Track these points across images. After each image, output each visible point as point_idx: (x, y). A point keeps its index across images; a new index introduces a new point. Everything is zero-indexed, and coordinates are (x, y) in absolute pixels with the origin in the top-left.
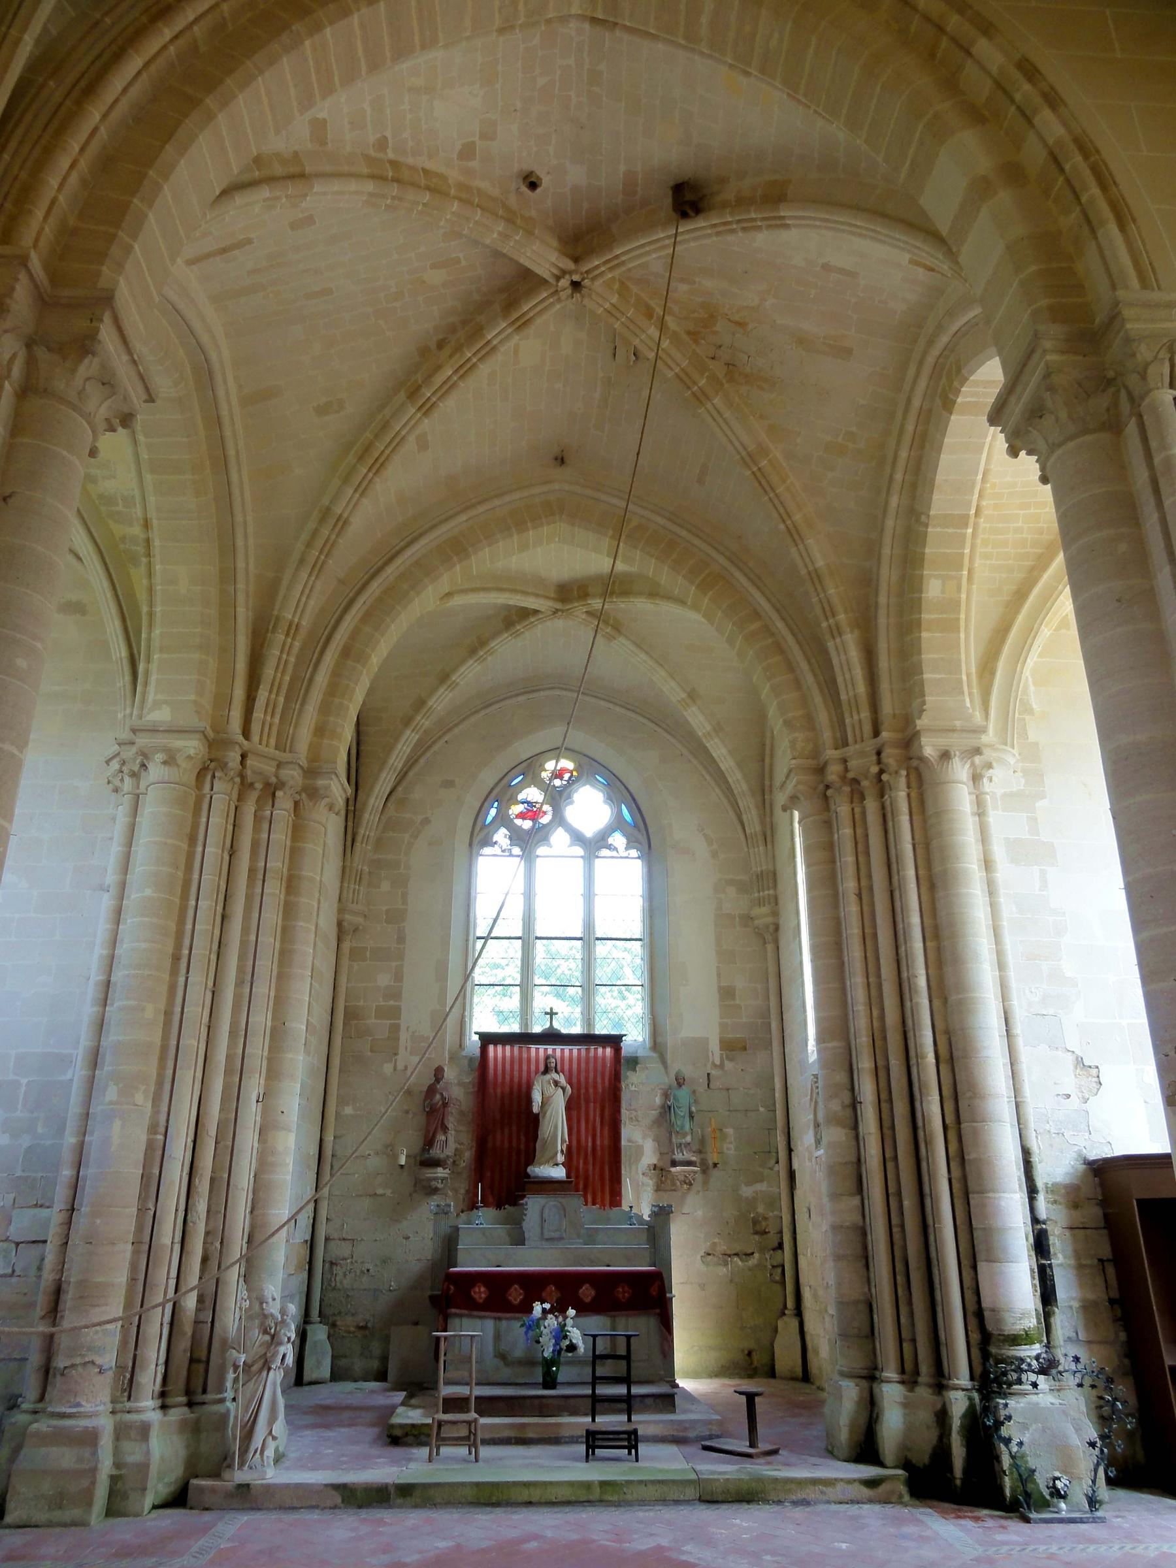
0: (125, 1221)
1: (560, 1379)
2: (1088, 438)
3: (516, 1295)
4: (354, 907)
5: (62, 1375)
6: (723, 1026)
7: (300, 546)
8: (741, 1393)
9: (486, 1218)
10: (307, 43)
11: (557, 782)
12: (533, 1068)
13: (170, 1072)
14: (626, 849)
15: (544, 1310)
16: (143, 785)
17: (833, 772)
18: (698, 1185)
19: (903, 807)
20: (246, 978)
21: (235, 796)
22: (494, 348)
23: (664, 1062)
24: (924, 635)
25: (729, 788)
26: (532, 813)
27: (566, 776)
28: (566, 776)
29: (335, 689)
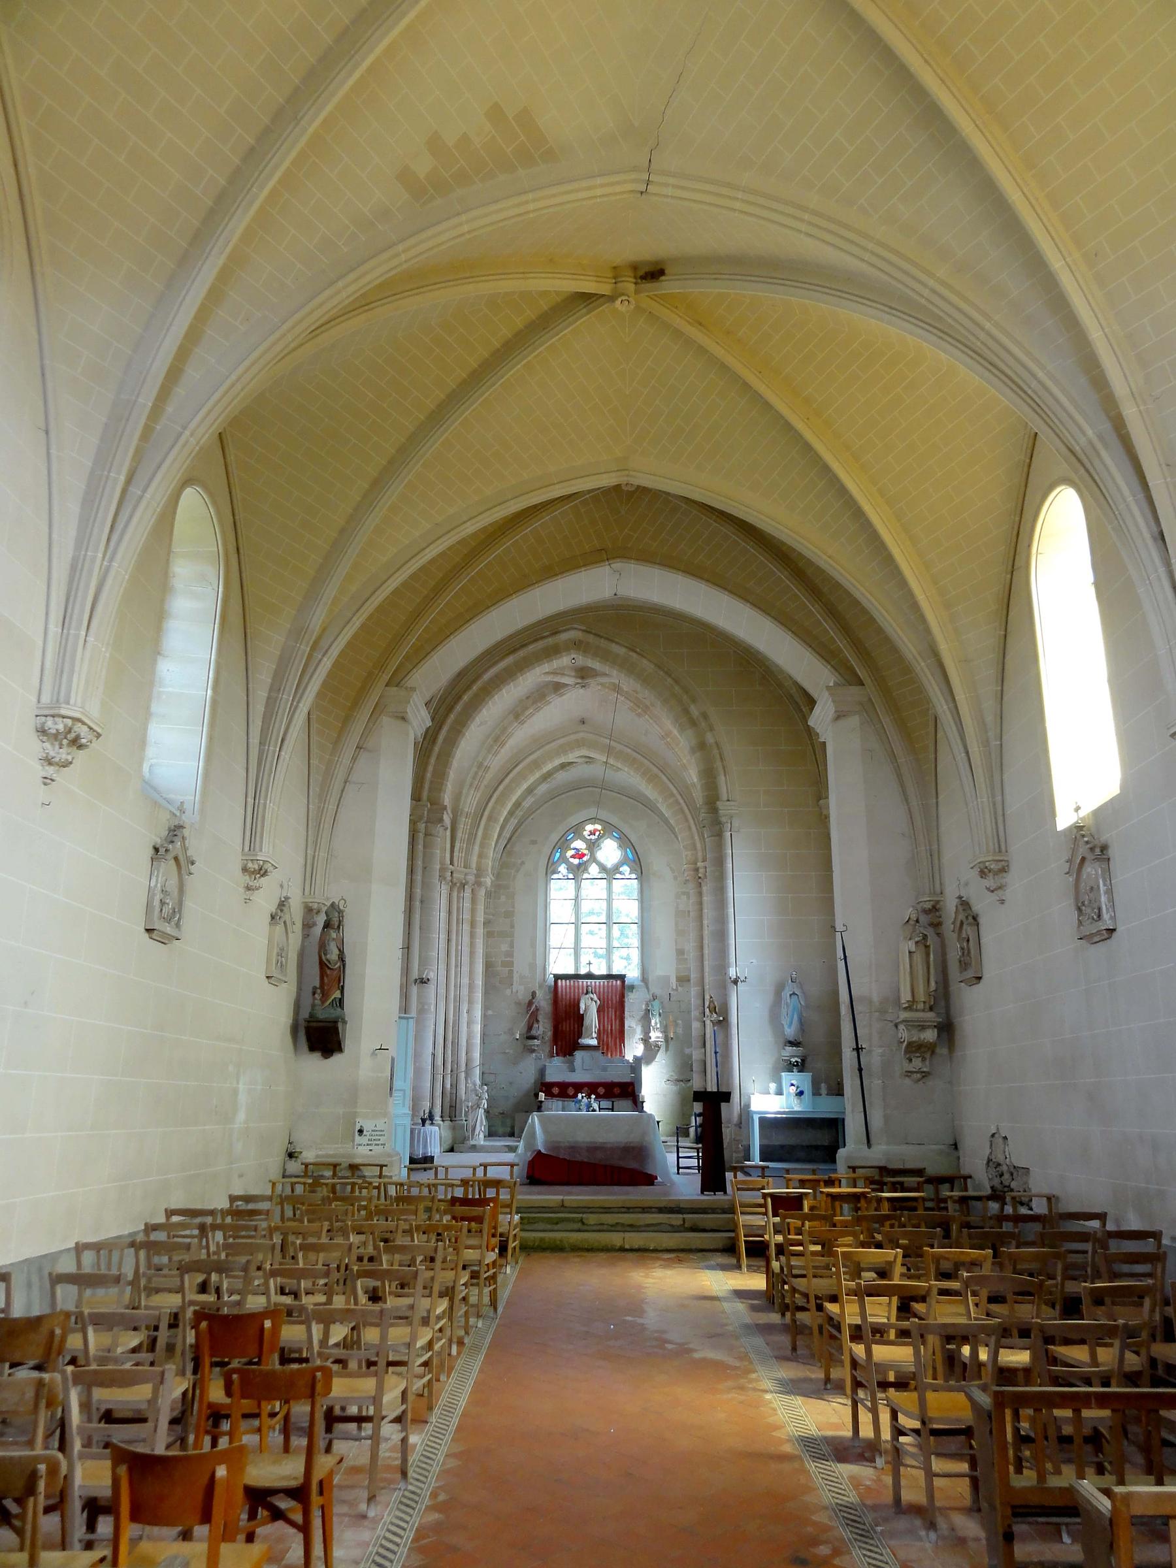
3: (571, 1091)
6: (677, 969)
7: (469, 780)
9: (558, 1061)
11: (593, 837)
20: (459, 965)
23: (648, 988)
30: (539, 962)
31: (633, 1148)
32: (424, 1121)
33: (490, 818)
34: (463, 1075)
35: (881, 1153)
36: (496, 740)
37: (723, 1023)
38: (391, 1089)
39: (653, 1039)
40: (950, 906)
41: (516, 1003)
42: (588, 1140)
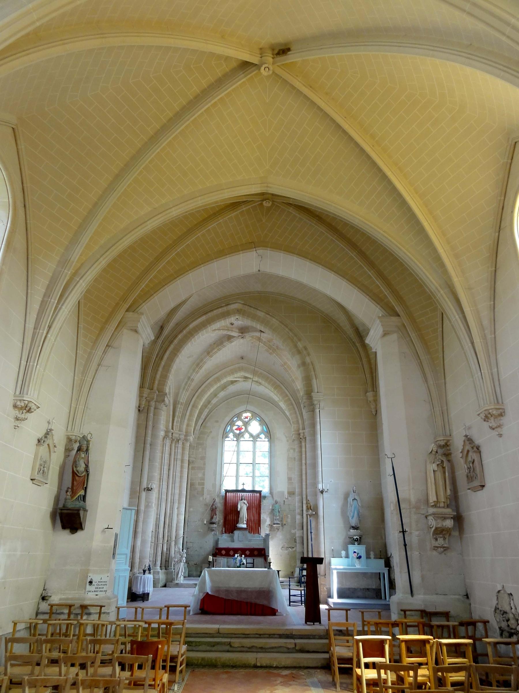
3: (231, 553)
7: (183, 384)
9: (225, 536)
11: (246, 420)
18: (280, 530)
20: (174, 482)
26: (239, 429)
27: (249, 418)
28: (249, 418)
30: (218, 483)
31: (264, 592)
32: (144, 571)
33: (193, 406)
34: (173, 544)
35: (420, 600)
36: (198, 365)
37: (316, 515)
38: (114, 554)
40: (458, 443)
41: (205, 505)
42: (237, 586)
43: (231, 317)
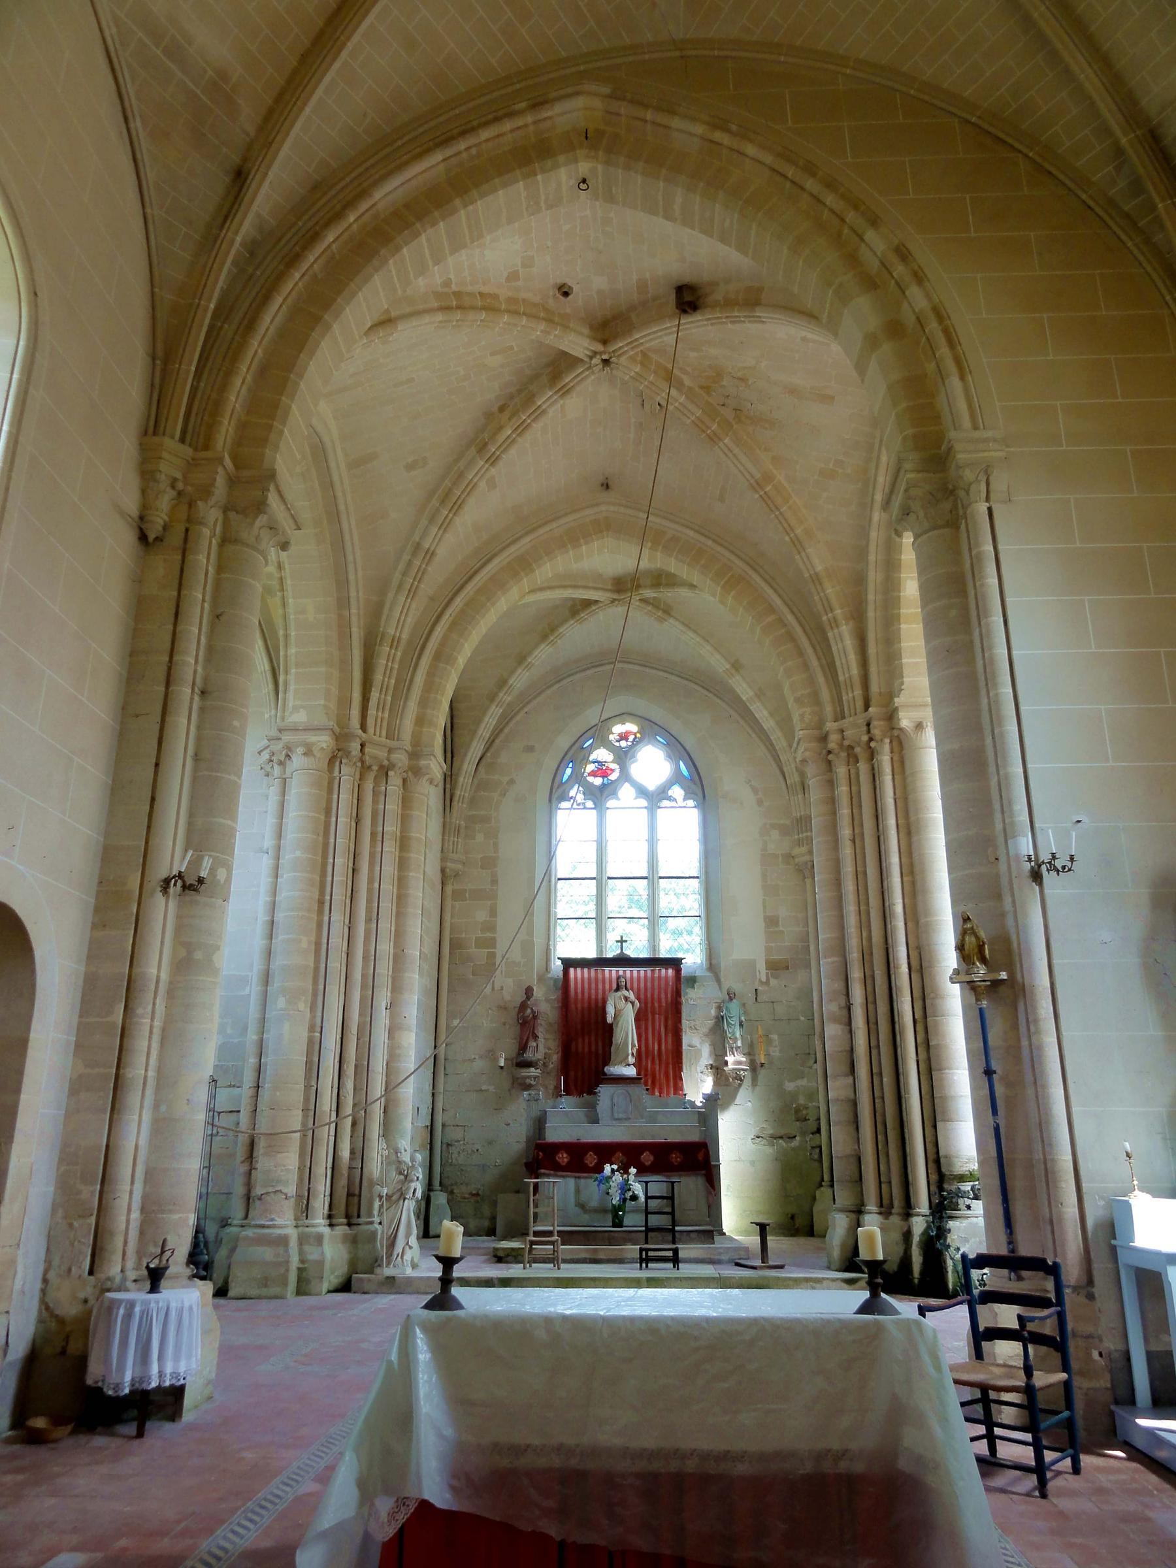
0: (296, 1095)
1: (626, 1222)
2: (936, 532)
3: (591, 1159)
4: (455, 856)
5: (260, 1199)
6: (768, 950)
7: (397, 575)
8: (757, 1224)
9: (568, 1104)
10: (391, 262)
11: (623, 744)
12: (607, 987)
13: (321, 987)
14: (684, 799)
15: (613, 1171)
16: (288, 770)
17: (833, 741)
19: (887, 769)
20: (373, 917)
21: (358, 776)
22: (544, 412)
23: (718, 981)
24: (903, 626)
25: (772, 745)
27: (631, 738)
28: (631, 738)
29: (430, 686)
30: (538, 940)
31: (850, 1482)
32: (155, 1278)
33: (438, 656)
39: (731, 1066)
41: (499, 1007)
42: (648, 1441)
43: (556, 166)
